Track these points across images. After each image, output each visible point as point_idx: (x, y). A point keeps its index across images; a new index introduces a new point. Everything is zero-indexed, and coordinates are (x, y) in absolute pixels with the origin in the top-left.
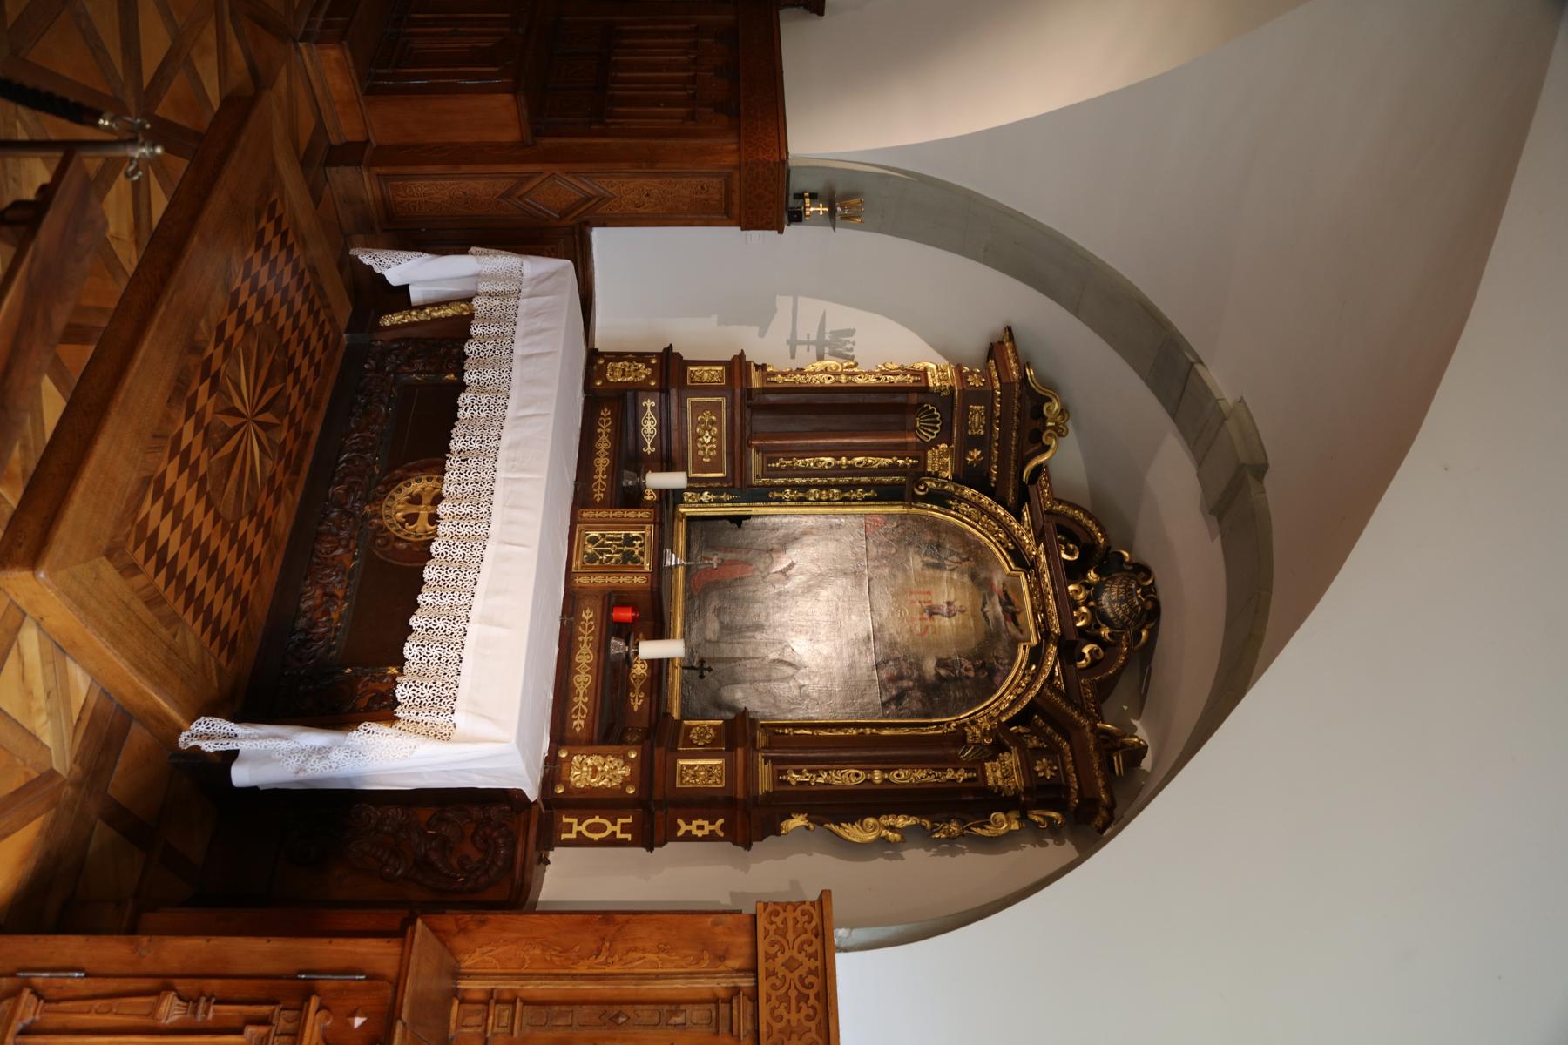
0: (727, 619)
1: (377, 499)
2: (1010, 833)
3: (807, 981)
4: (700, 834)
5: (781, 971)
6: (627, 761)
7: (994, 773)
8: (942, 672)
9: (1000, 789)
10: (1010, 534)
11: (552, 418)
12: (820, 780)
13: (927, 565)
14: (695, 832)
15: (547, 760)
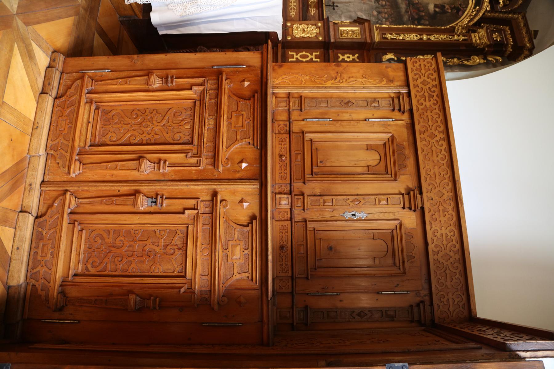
2: (479, 64)
3: (432, 90)
4: (348, 60)
5: (421, 85)
6: (318, 27)
7: (475, 38)
8: (437, 10)
9: (479, 45)
12: (401, 38)
14: (346, 59)
15: (283, 26)
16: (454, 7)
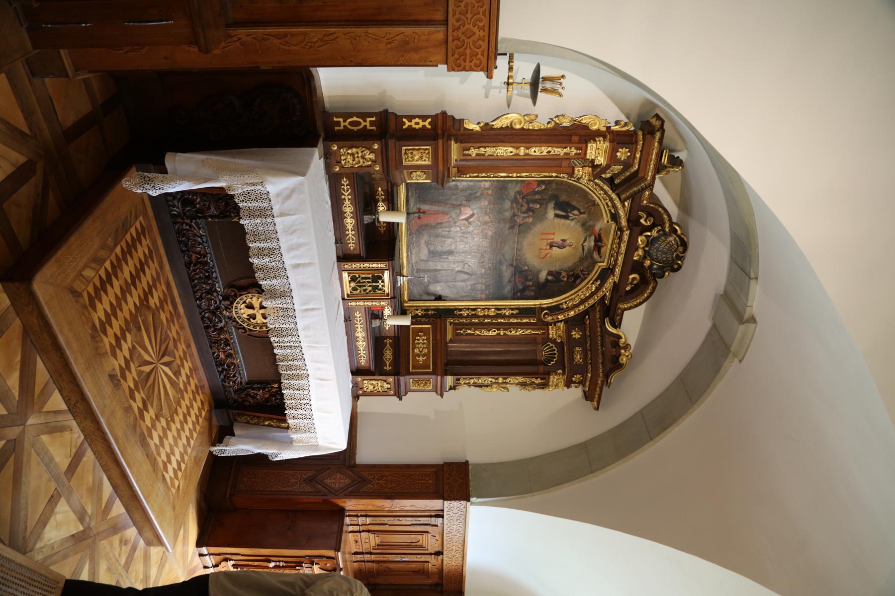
0: (432, 248)
1: (228, 308)
8: (550, 278)
10: (614, 206)
11: (324, 311)
13: (557, 216)
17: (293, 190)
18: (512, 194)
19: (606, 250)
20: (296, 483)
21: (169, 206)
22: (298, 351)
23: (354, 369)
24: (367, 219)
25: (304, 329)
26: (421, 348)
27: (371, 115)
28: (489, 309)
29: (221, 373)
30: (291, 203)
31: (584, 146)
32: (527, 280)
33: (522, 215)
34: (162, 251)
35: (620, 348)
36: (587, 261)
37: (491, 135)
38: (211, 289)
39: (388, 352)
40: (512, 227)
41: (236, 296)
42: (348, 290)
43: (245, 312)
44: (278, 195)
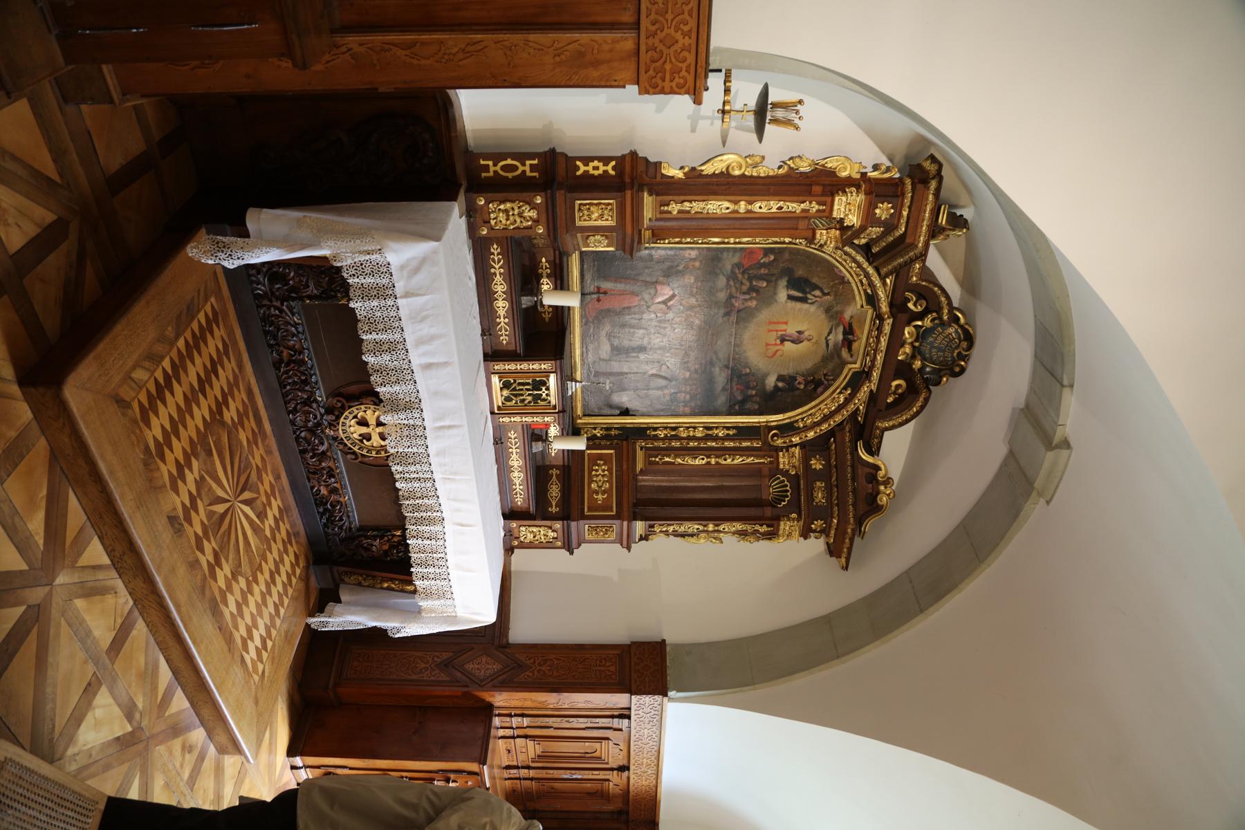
0: (616, 342)
1: (332, 425)
8: (780, 384)
10: (871, 284)
11: (466, 428)
13: (790, 298)
16: (812, 381)
17: (423, 261)
18: (729, 267)
19: (859, 346)
20: (426, 669)
21: (252, 282)
22: (429, 485)
23: (507, 511)
24: (526, 301)
25: (438, 454)
26: (600, 482)
27: (531, 156)
28: (695, 428)
29: (322, 515)
30: (419, 280)
31: (829, 199)
32: (748, 387)
33: (743, 297)
34: (242, 345)
35: (878, 483)
36: (832, 360)
37: (699, 184)
38: (309, 398)
39: (554, 487)
40: (727, 314)
41: (343, 409)
42: (498, 400)
43: (356, 431)
44: (402, 267)
